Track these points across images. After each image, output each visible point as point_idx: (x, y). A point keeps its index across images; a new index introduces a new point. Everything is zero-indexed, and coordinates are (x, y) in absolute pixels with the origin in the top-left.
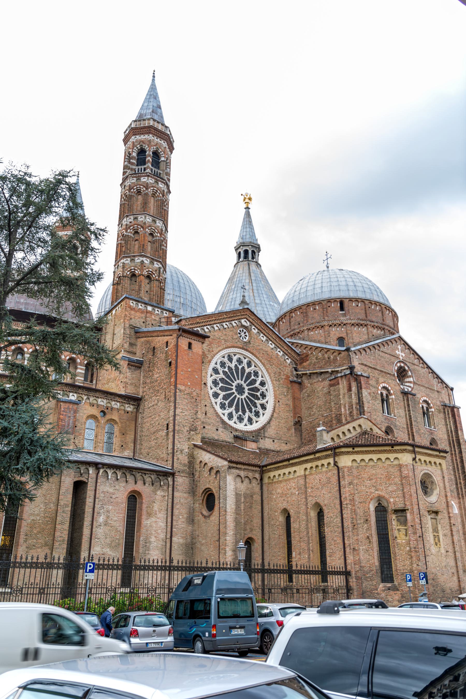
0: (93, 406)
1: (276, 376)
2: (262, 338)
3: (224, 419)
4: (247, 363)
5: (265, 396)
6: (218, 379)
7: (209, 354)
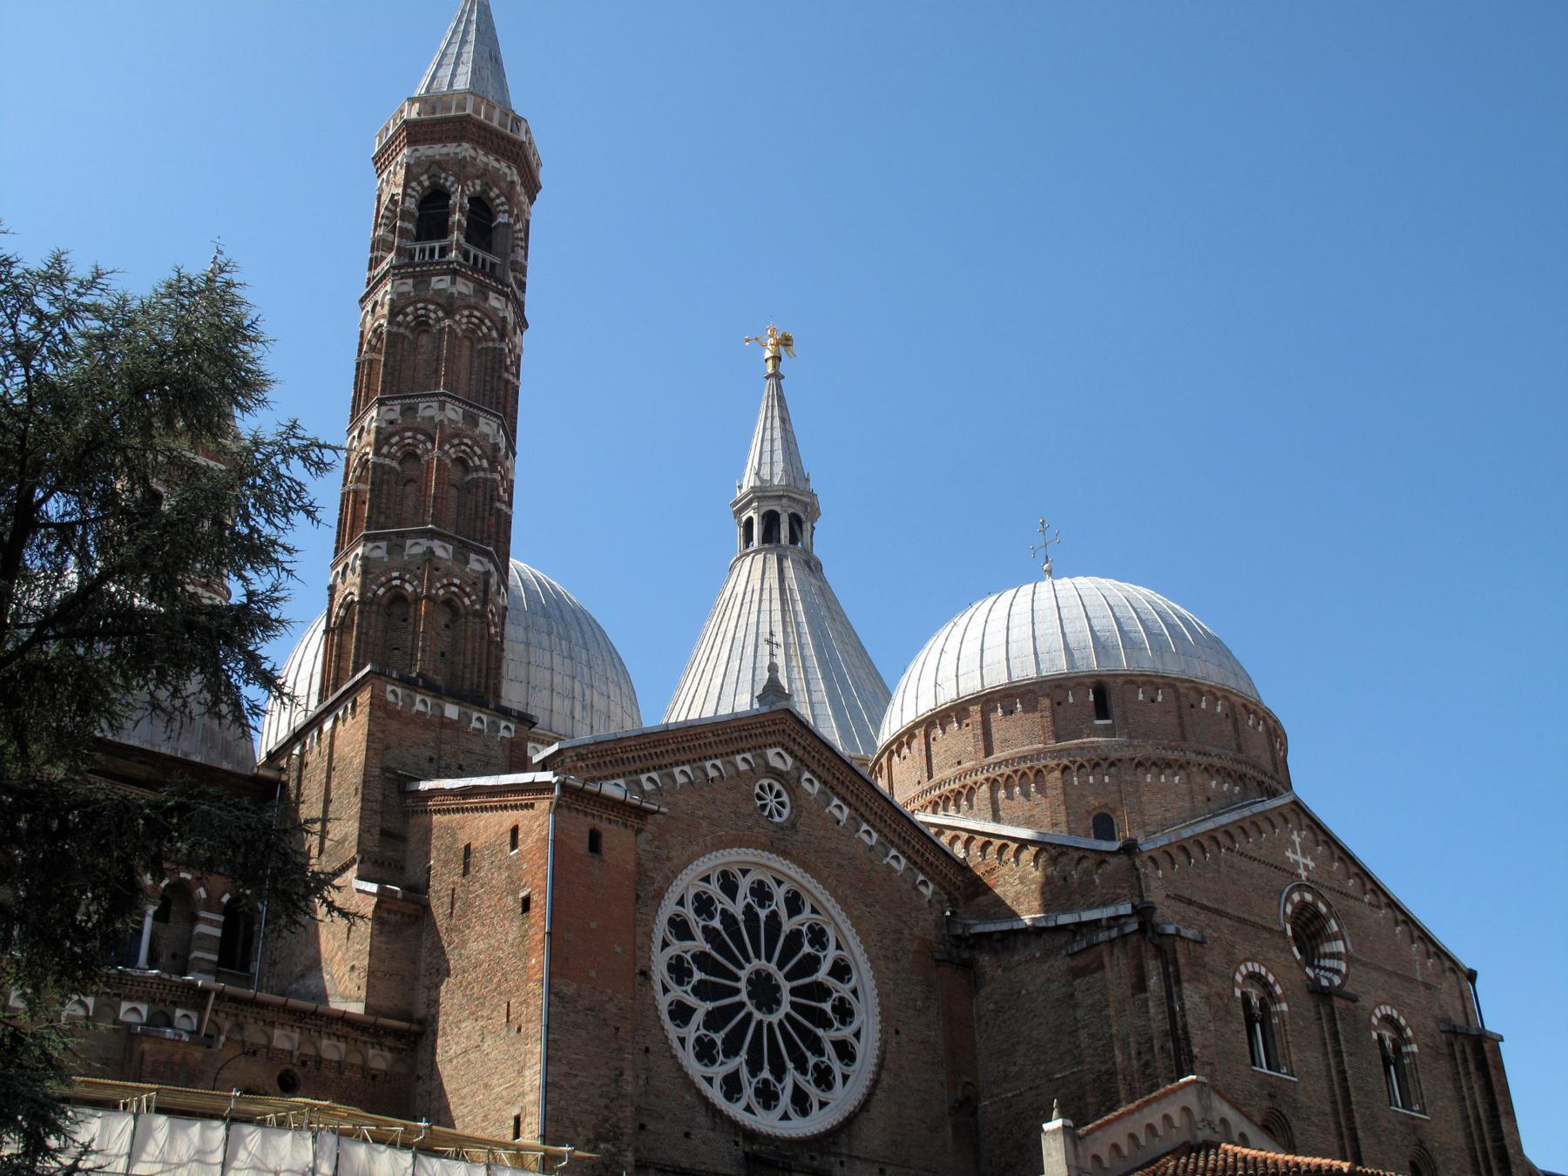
0: (254, 1053)
2: (836, 812)
3: (709, 1095)
4: (786, 900)
6: (688, 957)
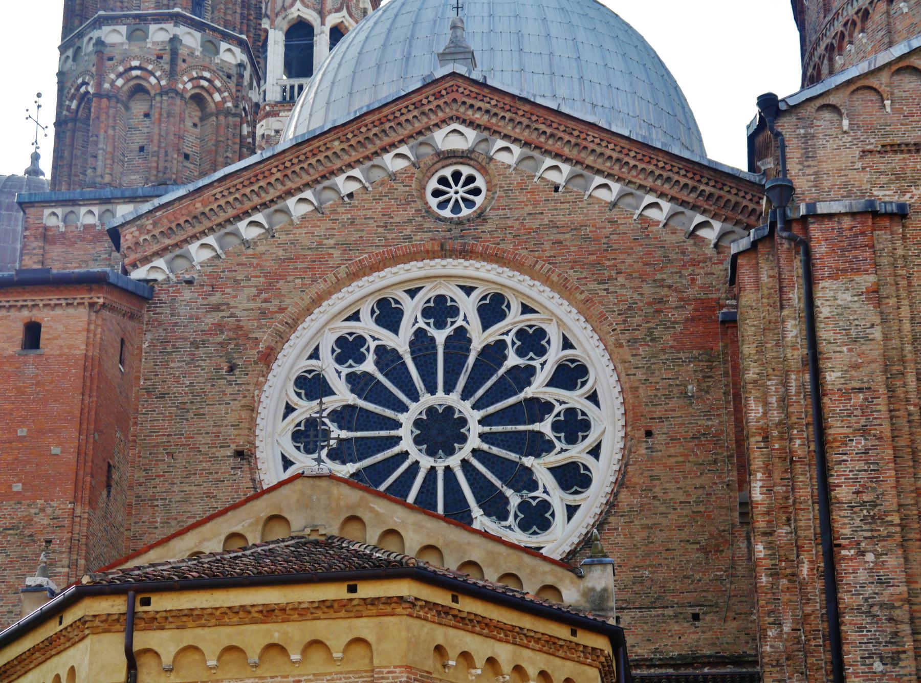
1: (637, 320)
2: (553, 176)
5: (586, 425)
7: (260, 327)
